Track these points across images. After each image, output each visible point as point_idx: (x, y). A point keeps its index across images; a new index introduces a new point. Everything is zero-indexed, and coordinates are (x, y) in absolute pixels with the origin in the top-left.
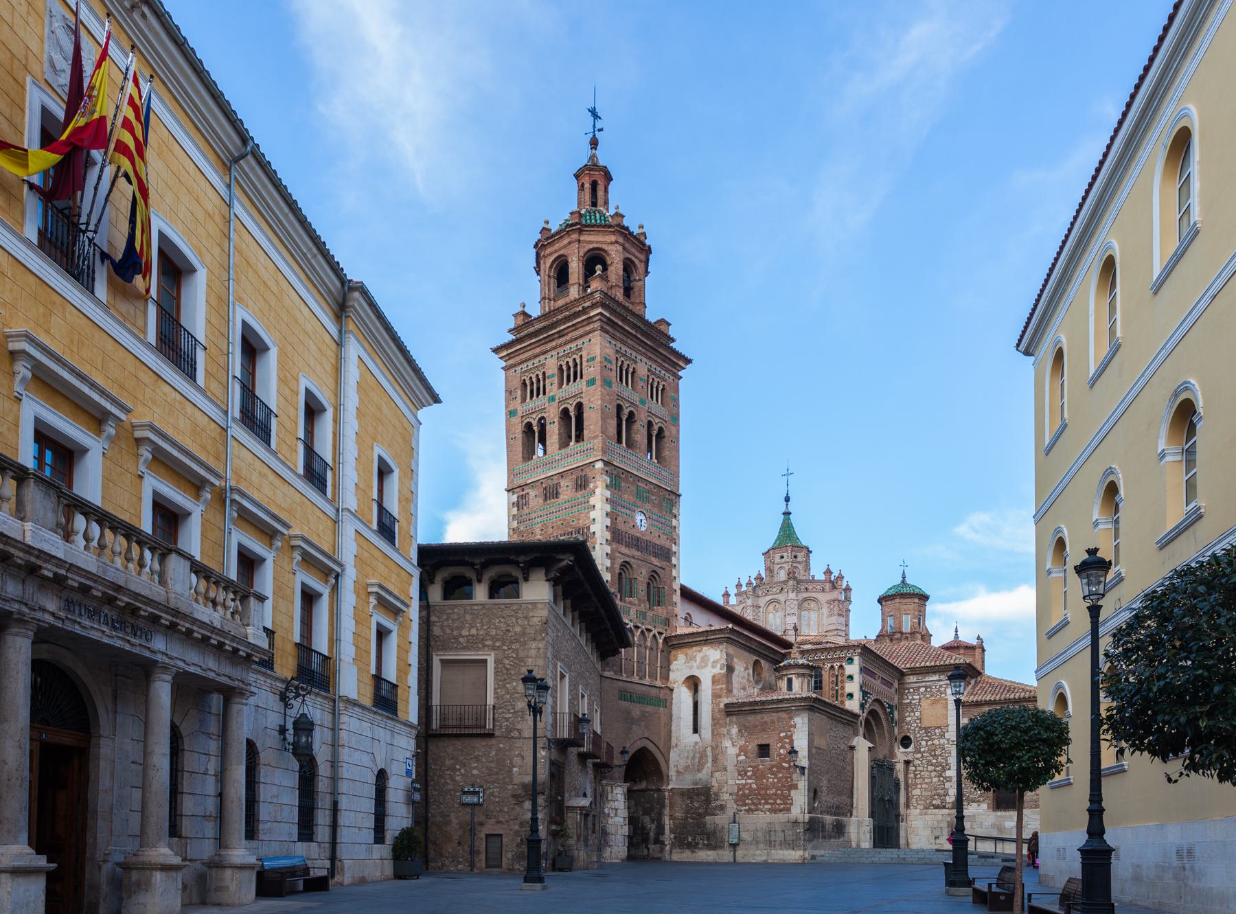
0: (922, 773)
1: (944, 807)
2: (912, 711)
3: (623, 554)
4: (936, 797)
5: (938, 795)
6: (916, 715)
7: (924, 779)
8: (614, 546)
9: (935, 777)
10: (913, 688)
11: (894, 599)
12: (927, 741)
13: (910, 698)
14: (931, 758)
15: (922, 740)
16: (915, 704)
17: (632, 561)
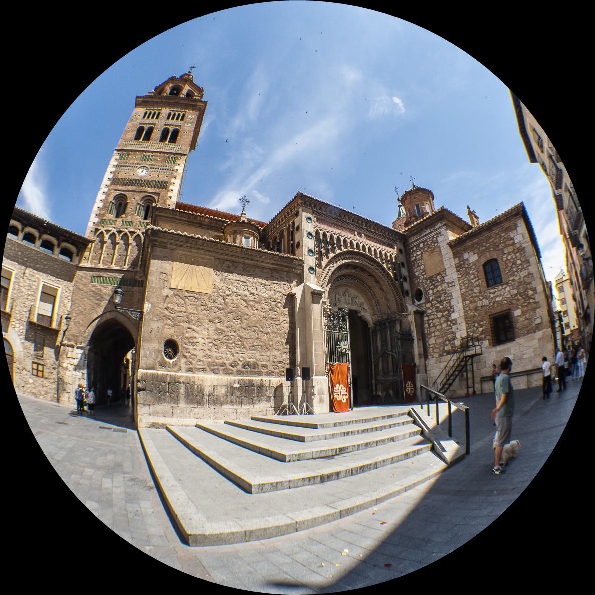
0: (434, 321)
1: (455, 352)
2: (419, 266)
3: (119, 190)
4: (447, 343)
5: (449, 340)
6: (421, 268)
7: (435, 327)
8: (112, 187)
9: (443, 323)
10: (414, 246)
11: (406, 198)
12: (433, 289)
13: (415, 255)
14: (438, 305)
15: (429, 289)
16: (419, 260)
17: (126, 194)
